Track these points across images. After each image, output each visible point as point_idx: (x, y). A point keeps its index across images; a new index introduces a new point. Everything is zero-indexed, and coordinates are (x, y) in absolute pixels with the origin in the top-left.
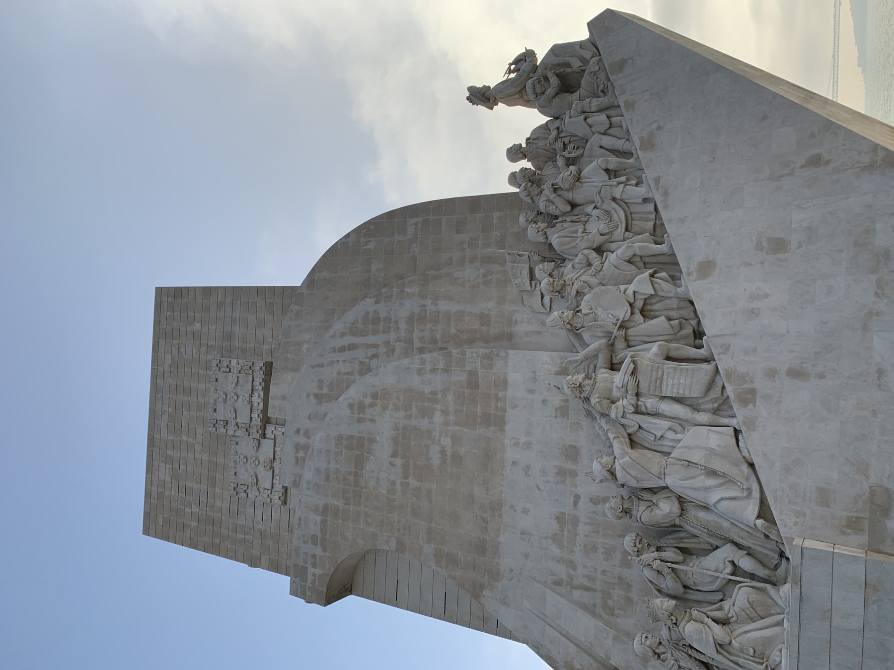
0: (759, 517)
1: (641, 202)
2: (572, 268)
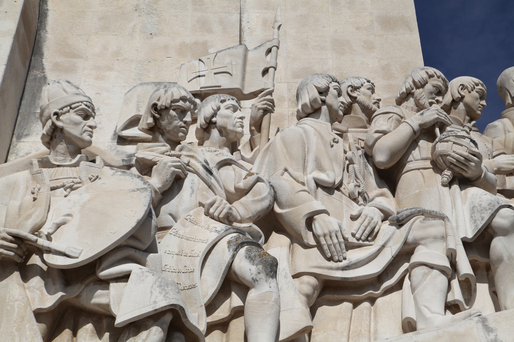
1: (403, 318)
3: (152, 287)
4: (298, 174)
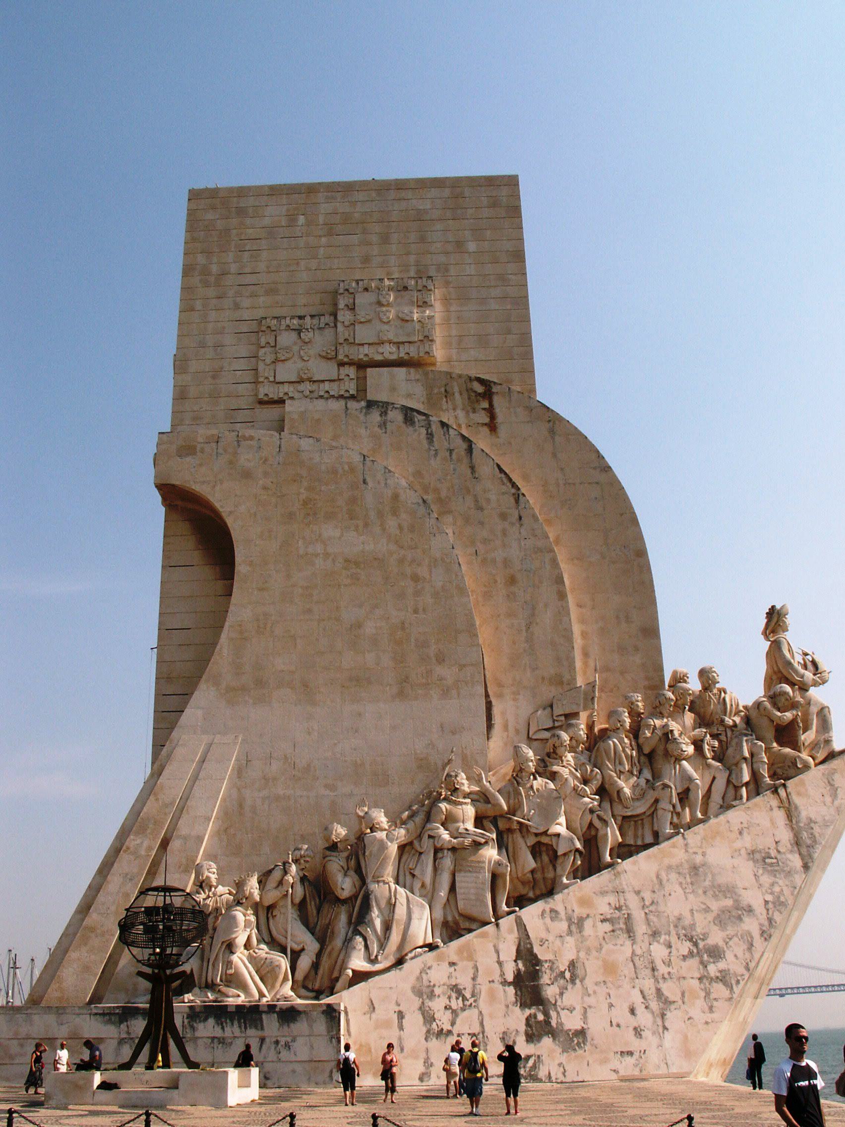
0: (353, 971)
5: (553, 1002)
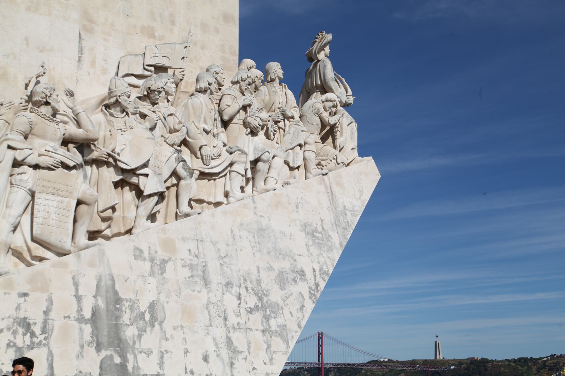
1: (225, 190)
2: (171, 113)
3: (157, 182)
4: (197, 124)
5: (131, 344)
